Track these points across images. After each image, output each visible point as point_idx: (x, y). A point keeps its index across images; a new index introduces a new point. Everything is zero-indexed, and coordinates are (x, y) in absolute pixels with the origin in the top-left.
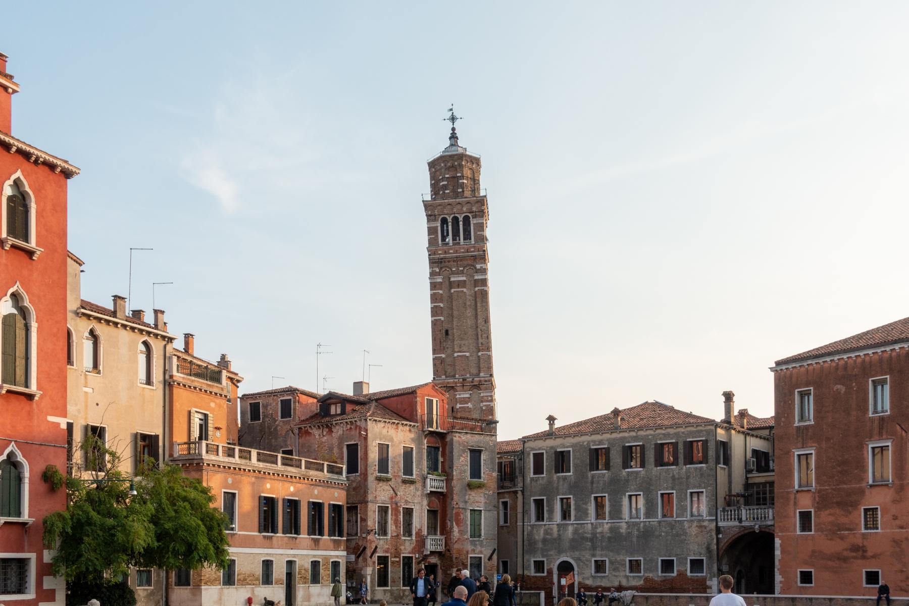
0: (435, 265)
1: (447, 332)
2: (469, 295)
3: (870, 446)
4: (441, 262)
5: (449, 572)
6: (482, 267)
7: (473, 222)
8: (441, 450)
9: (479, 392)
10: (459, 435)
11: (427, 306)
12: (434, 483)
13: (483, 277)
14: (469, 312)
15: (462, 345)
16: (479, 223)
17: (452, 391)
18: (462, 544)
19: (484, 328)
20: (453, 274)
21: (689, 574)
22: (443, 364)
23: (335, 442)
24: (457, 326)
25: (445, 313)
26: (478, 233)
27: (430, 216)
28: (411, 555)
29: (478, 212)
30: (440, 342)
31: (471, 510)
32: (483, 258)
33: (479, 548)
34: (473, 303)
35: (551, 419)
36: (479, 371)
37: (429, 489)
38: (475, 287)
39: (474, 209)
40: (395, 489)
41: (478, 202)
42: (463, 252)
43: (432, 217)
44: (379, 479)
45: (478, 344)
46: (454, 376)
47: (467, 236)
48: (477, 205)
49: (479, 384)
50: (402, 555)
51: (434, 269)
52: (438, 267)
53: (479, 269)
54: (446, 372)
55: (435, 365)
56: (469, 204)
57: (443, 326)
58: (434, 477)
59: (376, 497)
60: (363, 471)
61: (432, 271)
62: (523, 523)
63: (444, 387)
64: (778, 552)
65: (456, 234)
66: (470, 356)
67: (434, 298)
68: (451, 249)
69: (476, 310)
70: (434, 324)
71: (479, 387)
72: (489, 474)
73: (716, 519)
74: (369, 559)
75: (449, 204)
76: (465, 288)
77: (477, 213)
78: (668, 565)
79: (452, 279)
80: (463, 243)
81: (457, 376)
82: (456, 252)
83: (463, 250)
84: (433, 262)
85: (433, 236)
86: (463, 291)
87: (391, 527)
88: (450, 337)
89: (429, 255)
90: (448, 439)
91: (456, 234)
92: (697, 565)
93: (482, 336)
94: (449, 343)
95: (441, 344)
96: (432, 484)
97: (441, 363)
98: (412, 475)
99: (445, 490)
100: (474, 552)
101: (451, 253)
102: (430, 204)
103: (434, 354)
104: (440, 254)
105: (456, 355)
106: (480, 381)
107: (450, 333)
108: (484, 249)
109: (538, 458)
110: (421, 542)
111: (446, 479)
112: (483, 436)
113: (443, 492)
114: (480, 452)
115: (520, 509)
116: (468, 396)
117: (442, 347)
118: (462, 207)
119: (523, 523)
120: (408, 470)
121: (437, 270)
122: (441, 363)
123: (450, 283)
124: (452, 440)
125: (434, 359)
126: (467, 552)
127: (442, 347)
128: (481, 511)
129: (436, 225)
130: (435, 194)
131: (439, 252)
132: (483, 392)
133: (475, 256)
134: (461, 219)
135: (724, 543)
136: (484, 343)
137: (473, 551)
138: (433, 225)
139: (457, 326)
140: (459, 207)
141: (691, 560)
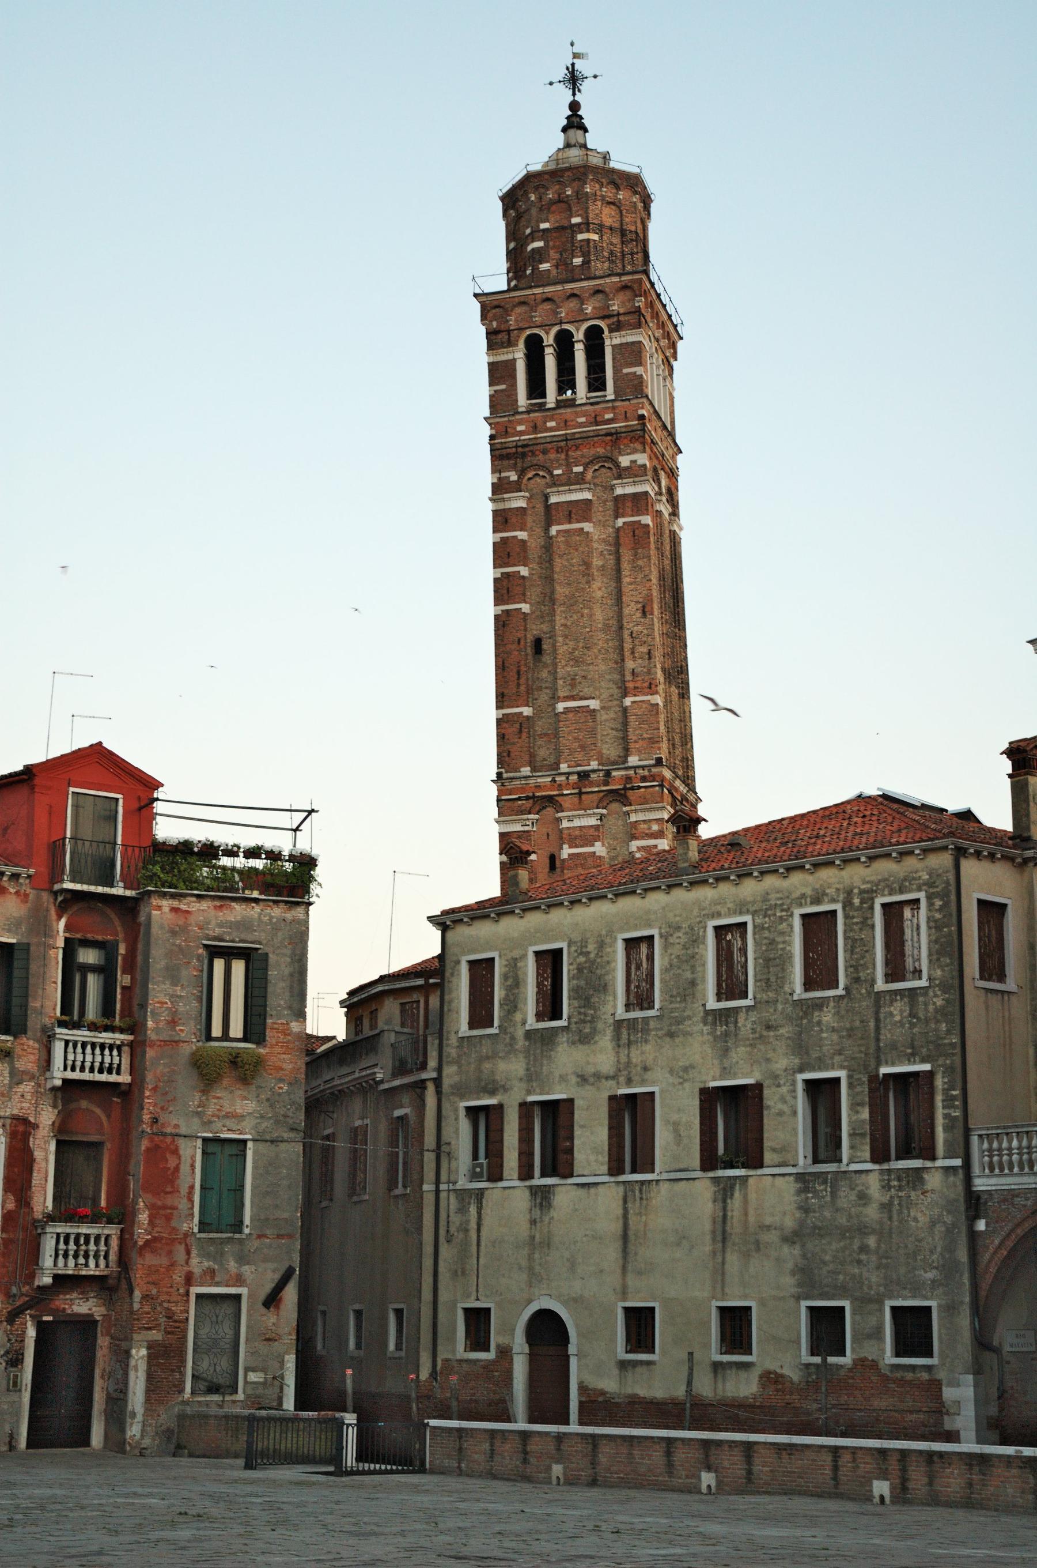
0: (506, 463)
2: (599, 540)
4: (523, 455)
6: (634, 462)
7: (611, 341)
9: (625, 809)
10: (175, 903)
14: (599, 588)
15: (578, 679)
16: (627, 343)
17: (550, 810)
18: (170, 1253)
19: (640, 628)
20: (554, 485)
21: (889, 1358)
22: (524, 736)
24: (565, 625)
25: (534, 593)
26: (625, 371)
29: (624, 314)
30: (518, 673)
31: (205, 1140)
33: (232, 1265)
34: (611, 561)
36: (627, 752)
37: (58, 1075)
38: (616, 518)
39: (615, 307)
42: (581, 425)
43: (500, 336)
47: (596, 382)
49: (625, 789)
51: (503, 475)
52: (514, 467)
53: (627, 468)
54: (532, 756)
55: (501, 738)
56: (600, 296)
57: (526, 630)
58: (82, 1035)
61: (499, 479)
62: (438, 1182)
63: (528, 798)
65: (566, 380)
66: (603, 708)
67: (503, 553)
68: (552, 419)
69: (618, 578)
70: (501, 623)
71: (625, 796)
73: (967, 1166)
75: (548, 300)
76: (587, 519)
77: (622, 318)
79: (553, 499)
80: (584, 401)
81: (564, 767)
83: (583, 420)
85: (503, 387)
86: (582, 529)
88: (547, 659)
89: (492, 437)
91: (566, 380)
93: (633, 653)
94: (544, 674)
95: (518, 679)
96: (71, 1057)
97: (520, 731)
99: (125, 1078)
100: (213, 1278)
101: (551, 429)
102: (496, 303)
103: (499, 706)
104: (522, 433)
105: (560, 707)
106: (628, 779)
108: (641, 412)
111: (131, 1045)
112: (257, 909)
113: (116, 1085)
116: (593, 821)
117: (523, 688)
118: (583, 304)
119: (438, 1182)
121: (514, 477)
122: (520, 731)
123: (548, 508)
124: (149, 916)
125: (499, 722)
126: (189, 1280)
127: (523, 688)
128: (244, 1142)
129: (510, 357)
130: (516, 277)
131: (520, 428)
132: (636, 811)
133: (617, 433)
135: (991, 1249)
136: (638, 670)
138: (503, 356)
139: (565, 625)
140: (573, 304)
141: (894, 1309)
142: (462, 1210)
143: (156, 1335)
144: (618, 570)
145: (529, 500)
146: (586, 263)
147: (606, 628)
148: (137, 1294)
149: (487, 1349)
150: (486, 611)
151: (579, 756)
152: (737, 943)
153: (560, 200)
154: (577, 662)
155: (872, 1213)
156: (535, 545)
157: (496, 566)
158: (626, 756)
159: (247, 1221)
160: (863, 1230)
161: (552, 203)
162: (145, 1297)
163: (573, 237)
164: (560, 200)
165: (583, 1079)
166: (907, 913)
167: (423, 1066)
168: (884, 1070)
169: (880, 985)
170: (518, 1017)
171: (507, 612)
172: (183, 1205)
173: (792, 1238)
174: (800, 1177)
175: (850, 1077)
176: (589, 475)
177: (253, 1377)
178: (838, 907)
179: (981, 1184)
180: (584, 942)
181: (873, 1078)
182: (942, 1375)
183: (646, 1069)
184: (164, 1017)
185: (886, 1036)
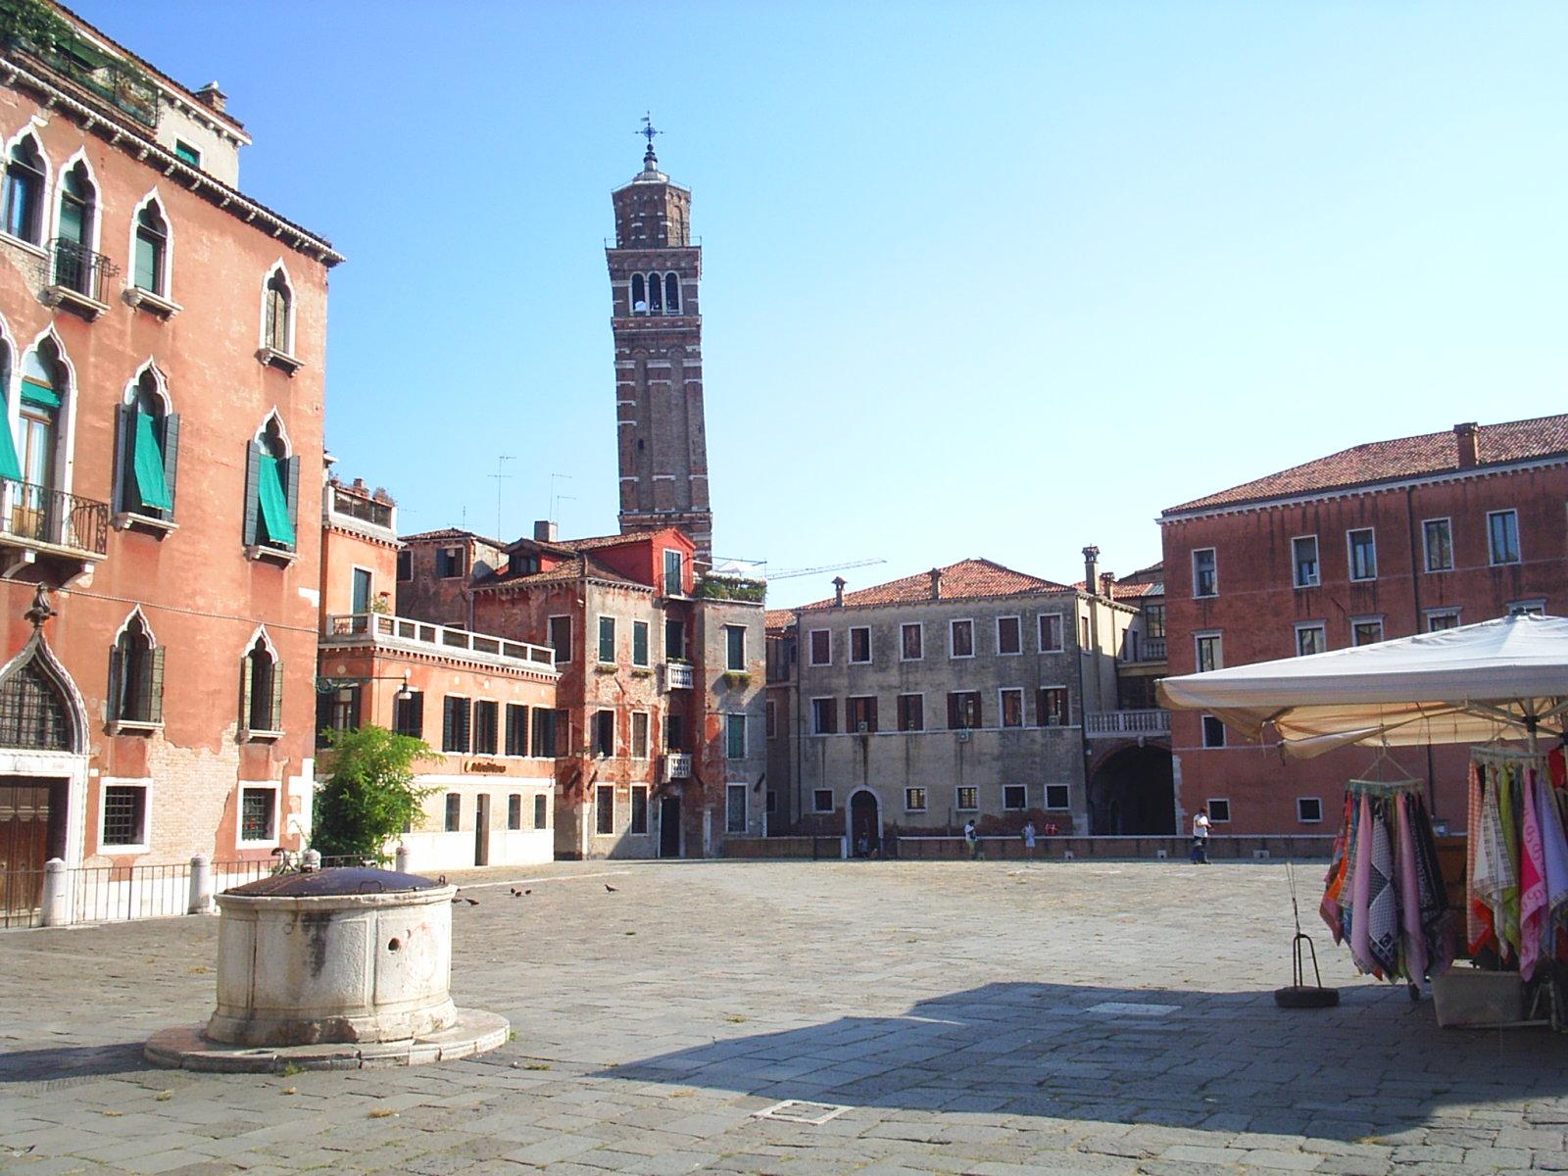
1: (641, 443)
3: (1297, 628)
4: (633, 340)
5: (697, 810)
7: (681, 283)
8: (685, 626)
11: (612, 403)
12: (675, 678)
13: (697, 365)
14: (676, 415)
20: (651, 358)
23: (533, 612)
27: (617, 270)
28: (643, 785)
32: (696, 336)
33: (742, 773)
34: (681, 402)
35: (839, 583)
38: (685, 378)
39: (683, 265)
40: (624, 684)
41: (688, 254)
42: (665, 327)
44: (600, 671)
45: (688, 461)
46: (651, 510)
47: (674, 304)
48: (687, 259)
50: (632, 785)
52: (628, 346)
55: (622, 493)
59: (596, 697)
60: (577, 658)
62: (799, 738)
64: (1177, 775)
67: (622, 392)
70: (622, 430)
72: (755, 661)
73: (1083, 728)
74: (585, 789)
78: (1015, 797)
79: (649, 366)
82: (656, 325)
84: (620, 339)
87: (617, 742)
88: (646, 451)
89: (614, 329)
90: (697, 611)
92: (1058, 796)
98: (646, 664)
99: (691, 687)
104: (631, 328)
105: (655, 478)
106: (692, 518)
107: (645, 444)
109: (821, 639)
110: (659, 764)
111: (693, 671)
114: (742, 629)
115: (793, 714)
117: (634, 468)
120: (641, 656)
123: (646, 370)
124: (703, 612)
126: (726, 780)
130: (623, 239)
134: (663, 278)
137: (734, 776)
138: (621, 284)
140: (660, 260)
142: (813, 746)
143: (714, 805)
144: (686, 408)
145: (636, 364)
146: (666, 238)
147: (679, 438)
148: (706, 786)
149: (830, 809)
150: (612, 424)
151: (666, 505)
152: (965, 630)
153: (651, 199)
154: (664, 455)
155: (1037, 747)
156: (639, 389)
157: (618, 399)
158: (691, 505)
159: (746, 749)
160: (1032, 755)
161: (646, 202)
162: (710, 788)
163: (658, 223)
164: (651, 199)
165: (882, 688)
166: (1052, 621)
167: (787, 679)
168: (1042, 688)
169: (1040, 651)
170: (844, 659)
171: (624, 425)
172: (722, 745)
173: (996, 759)
174: (1000, 732)
175: (1025, 690)
176: (669, 355)
177: (751, 823)
178: (1019, 617)
179: (1089, 735)
180: (881, 626)
181: (1038, 691)
182: (1073, 814)
183: (917, 684)
184: (712, 658)
185: (1043, 673)
